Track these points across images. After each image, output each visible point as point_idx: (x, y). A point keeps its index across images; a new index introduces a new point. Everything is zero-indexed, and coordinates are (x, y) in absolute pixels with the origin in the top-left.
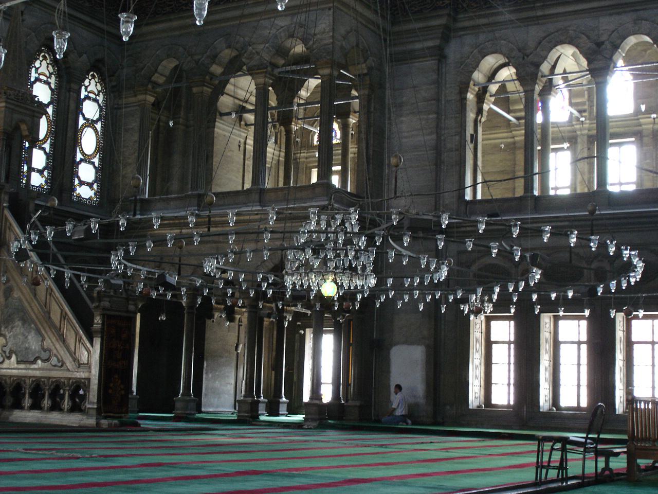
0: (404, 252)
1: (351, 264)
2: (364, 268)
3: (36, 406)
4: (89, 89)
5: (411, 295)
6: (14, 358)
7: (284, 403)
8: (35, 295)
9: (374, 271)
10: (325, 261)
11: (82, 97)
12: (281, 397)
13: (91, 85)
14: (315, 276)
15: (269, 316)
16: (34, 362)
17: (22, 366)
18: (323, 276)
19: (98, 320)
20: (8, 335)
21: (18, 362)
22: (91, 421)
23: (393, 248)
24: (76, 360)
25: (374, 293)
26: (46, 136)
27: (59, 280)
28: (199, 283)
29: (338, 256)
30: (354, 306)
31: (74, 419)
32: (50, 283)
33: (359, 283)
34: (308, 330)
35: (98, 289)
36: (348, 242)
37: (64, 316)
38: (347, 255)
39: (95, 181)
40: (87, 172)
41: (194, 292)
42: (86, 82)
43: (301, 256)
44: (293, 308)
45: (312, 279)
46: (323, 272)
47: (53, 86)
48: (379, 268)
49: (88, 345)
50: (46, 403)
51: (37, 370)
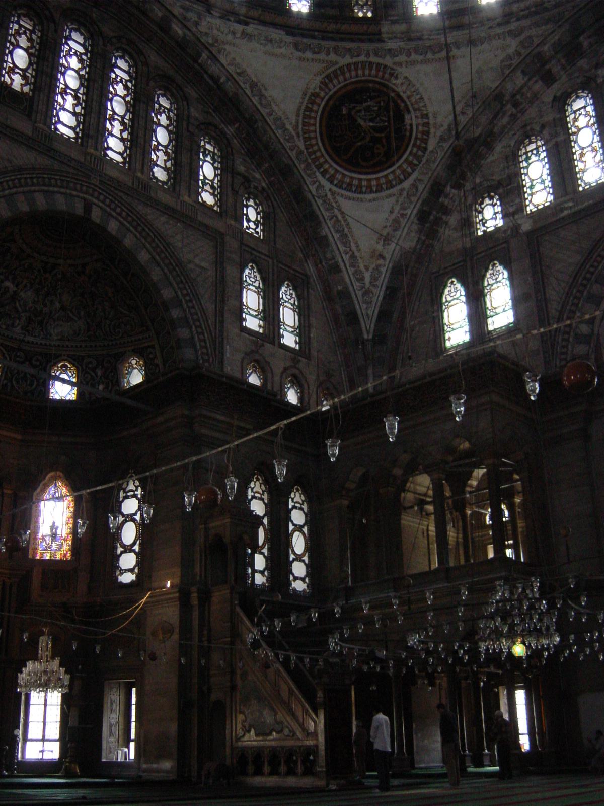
0: (582, 610)
1: (535, 626)
2: (548, 628)
3: (274, 772)
4: (295, 500)
5: (592, 648)
6: (252, 732)
7: (487, 754)
8: (266, 677)
9: (557, 630)
10: (512, 627)
11: (290, 507)
12: (484, 750)
13: (296, 497)
14: (506, 640)
15: (466, 678)
16: (270, 734)
17: (261, 738)
18: (513, 639)
19: (320, 694)
20: (246, 712)
21: (257, 735)
22: (321, 783)
23: (572, 608)
24: (304, 730)
25: (559, 649)
26: (264, 543)
27: (286, 663)
28: (404, 655)
29: (523, 620)
30: (541, 662)
31: (307, 782)
32: (278, 666)
33: (545, 642)
34: (500, 688)
35: (318, 667)
36: (531, 607)
37: (291, 692)
38: (531, 619)
39: (306, 576)
40: (299, 569)
41: (400, 663)
42: (292, 495)
43: (490, 624)
44: (486, 670)
45: (503, 643)
46: (512, 637)
47: (266, 501)
48: (562, 628)
49: (314, 716)
50: (283, 768)
51: (273, 739)
